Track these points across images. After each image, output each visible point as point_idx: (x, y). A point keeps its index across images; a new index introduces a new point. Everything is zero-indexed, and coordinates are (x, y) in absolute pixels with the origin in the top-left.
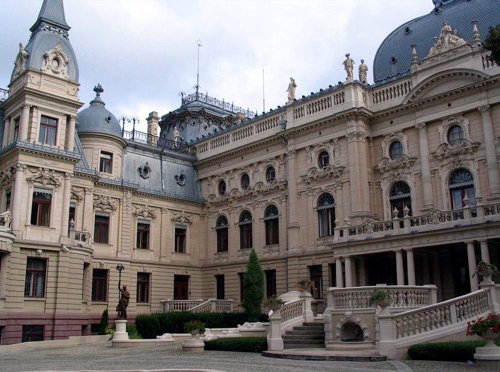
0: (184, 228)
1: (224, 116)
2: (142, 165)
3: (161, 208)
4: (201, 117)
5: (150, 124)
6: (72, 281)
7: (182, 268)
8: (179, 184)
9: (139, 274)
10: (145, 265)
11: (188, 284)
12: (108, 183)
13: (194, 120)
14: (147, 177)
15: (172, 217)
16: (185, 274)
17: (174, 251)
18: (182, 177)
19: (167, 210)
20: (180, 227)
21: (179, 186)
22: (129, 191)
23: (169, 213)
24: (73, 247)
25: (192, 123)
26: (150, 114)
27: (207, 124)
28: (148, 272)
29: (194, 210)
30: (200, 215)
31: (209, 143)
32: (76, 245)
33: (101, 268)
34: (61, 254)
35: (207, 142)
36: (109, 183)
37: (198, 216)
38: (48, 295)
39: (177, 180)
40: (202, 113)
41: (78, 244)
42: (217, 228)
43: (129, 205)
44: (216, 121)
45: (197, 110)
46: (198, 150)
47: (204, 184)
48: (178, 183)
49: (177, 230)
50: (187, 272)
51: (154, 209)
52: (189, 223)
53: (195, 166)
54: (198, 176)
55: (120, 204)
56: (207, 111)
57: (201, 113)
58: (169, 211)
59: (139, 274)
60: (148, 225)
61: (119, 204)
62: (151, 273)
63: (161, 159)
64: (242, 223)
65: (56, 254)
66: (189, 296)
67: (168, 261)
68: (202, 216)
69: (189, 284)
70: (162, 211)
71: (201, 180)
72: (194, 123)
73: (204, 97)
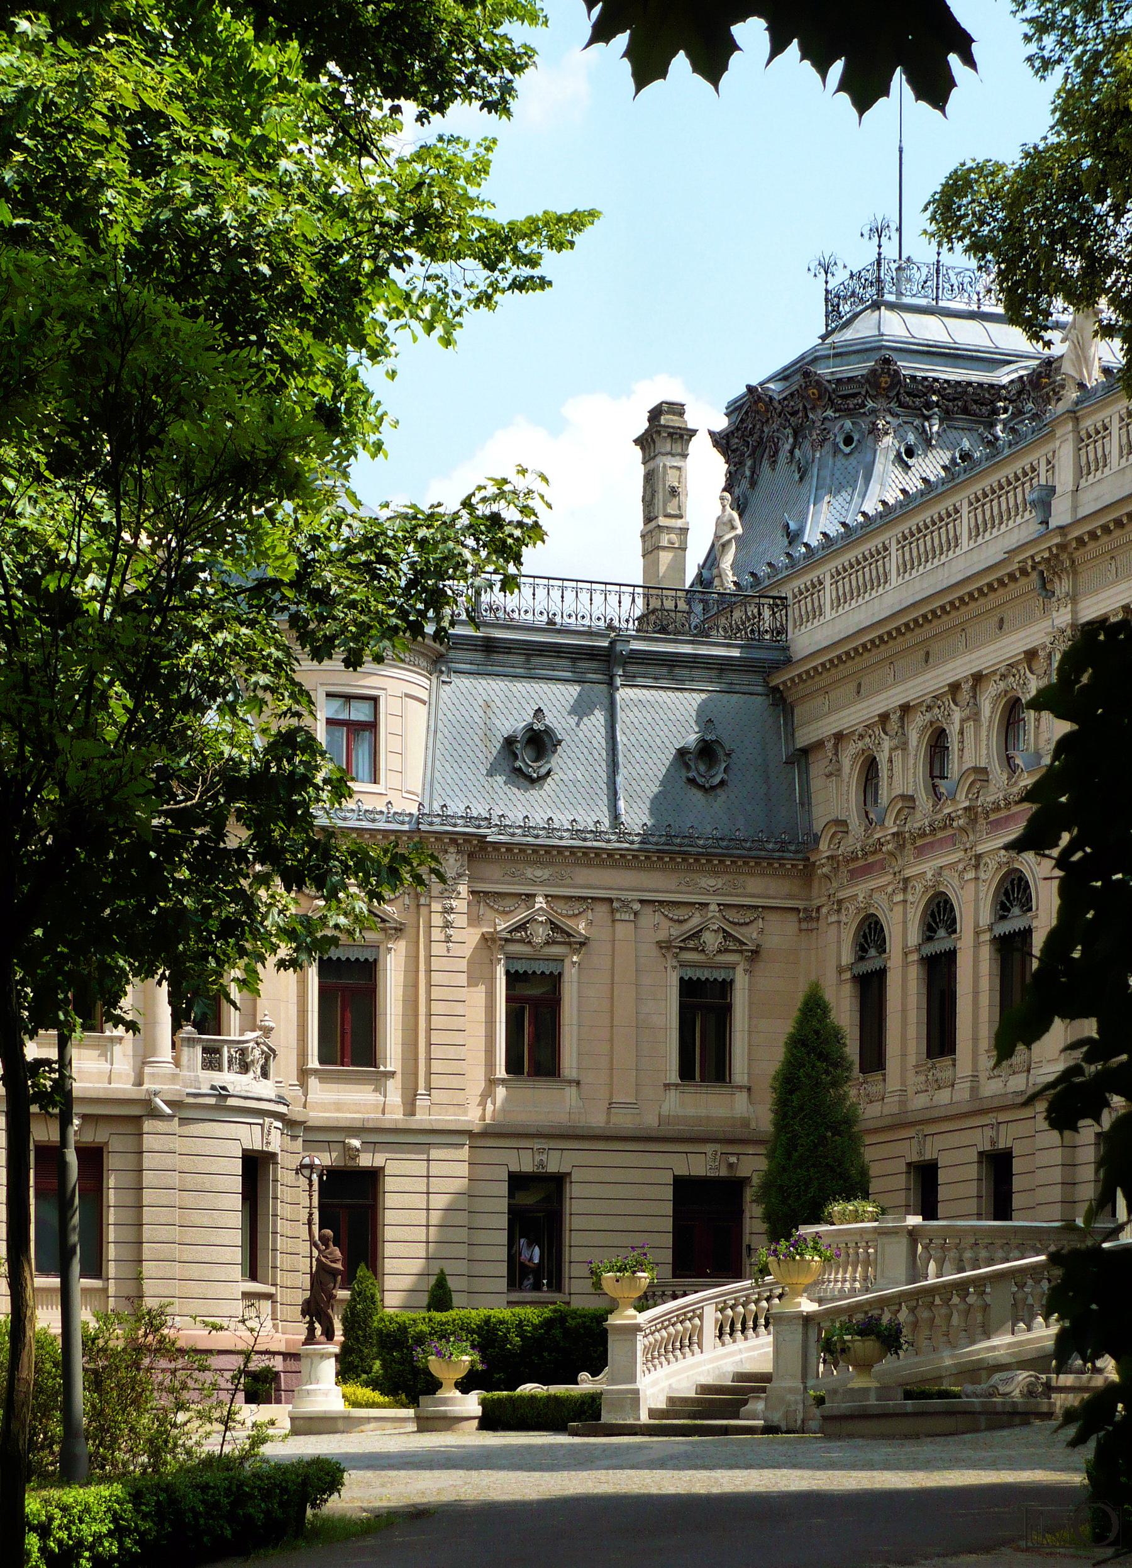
0: (720, 975)
1: (1004, 376)
2: (515, 722)
3: (610, 900)
4: (880, 404)
5: (651, 465)
6: (176, 1216)
7: (709, 1148)
8: (701, 787)
9: (517, 1182)
10: (537, 1144)
11: (742, 1212)
12: (357, 824)
13: (848, 424)
14: (543, 771)
15: (662, 935)
16: (723, 1172)
17: (674, 1077)
18: (707, 751)
19: (637, 906)
20: (704, 975)
21: (697, 795)
22: (452, 849)
23: (649, 918)
24: (191, 1100)
25: (840, 440)
26: (655, 414)
27: (911, 438)
28: (552, 1168)
29: (772, 892)
30: (797, 910)
31: (828, 582)
32: (205, 1090)
33: (350, 1163)
34: (148, 1125)
35: (818, 572)
36: (365, 824)
37: (792, 917)
38: (112, 1269)
39: (688, 767)
40: (885, 381)
41: (213, 1088)
42: (855, 971)
43: (454, 903)
44: (965, 411)
45: (859, 368)
46: (794, 612)
47: (818, 767)
48: (692, 781)
49: (688, 988)
50: (731, 1166)
51: (578, 907)
52: (741, 952)
53: (775, 689)
54: (791, 735)
55: (418, 906)
56: (907, 367)
57: (876, 385)
58: (648, 910)
59: (517, 1182)
60: (555, 980)
61: (413, 909)
62: (569, 1174)
63: (611, 683)
64: (930, 949)
65: (130, 1129)
66: (746, 1261)
67: (650, 1121)
68: (808, 917)
69: (747, 1214)
70: (613, 911)
71: (805, 752)
72: (848, 441)
73: (919, 276)
